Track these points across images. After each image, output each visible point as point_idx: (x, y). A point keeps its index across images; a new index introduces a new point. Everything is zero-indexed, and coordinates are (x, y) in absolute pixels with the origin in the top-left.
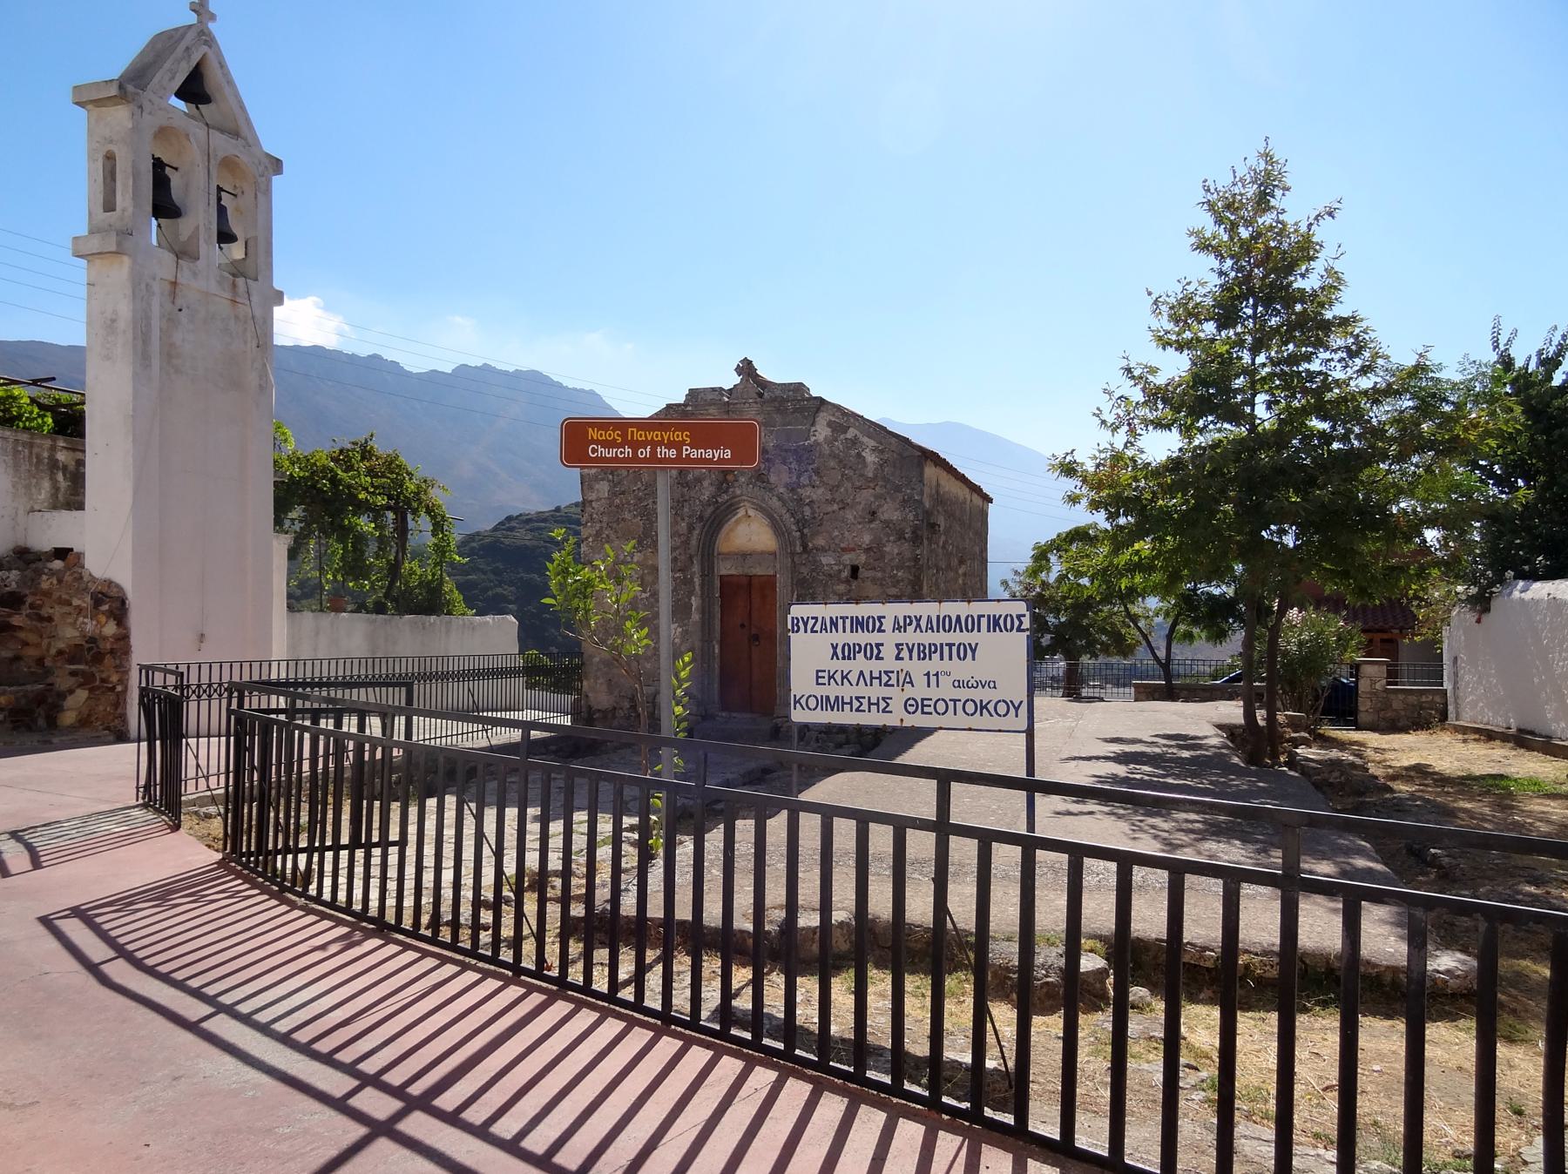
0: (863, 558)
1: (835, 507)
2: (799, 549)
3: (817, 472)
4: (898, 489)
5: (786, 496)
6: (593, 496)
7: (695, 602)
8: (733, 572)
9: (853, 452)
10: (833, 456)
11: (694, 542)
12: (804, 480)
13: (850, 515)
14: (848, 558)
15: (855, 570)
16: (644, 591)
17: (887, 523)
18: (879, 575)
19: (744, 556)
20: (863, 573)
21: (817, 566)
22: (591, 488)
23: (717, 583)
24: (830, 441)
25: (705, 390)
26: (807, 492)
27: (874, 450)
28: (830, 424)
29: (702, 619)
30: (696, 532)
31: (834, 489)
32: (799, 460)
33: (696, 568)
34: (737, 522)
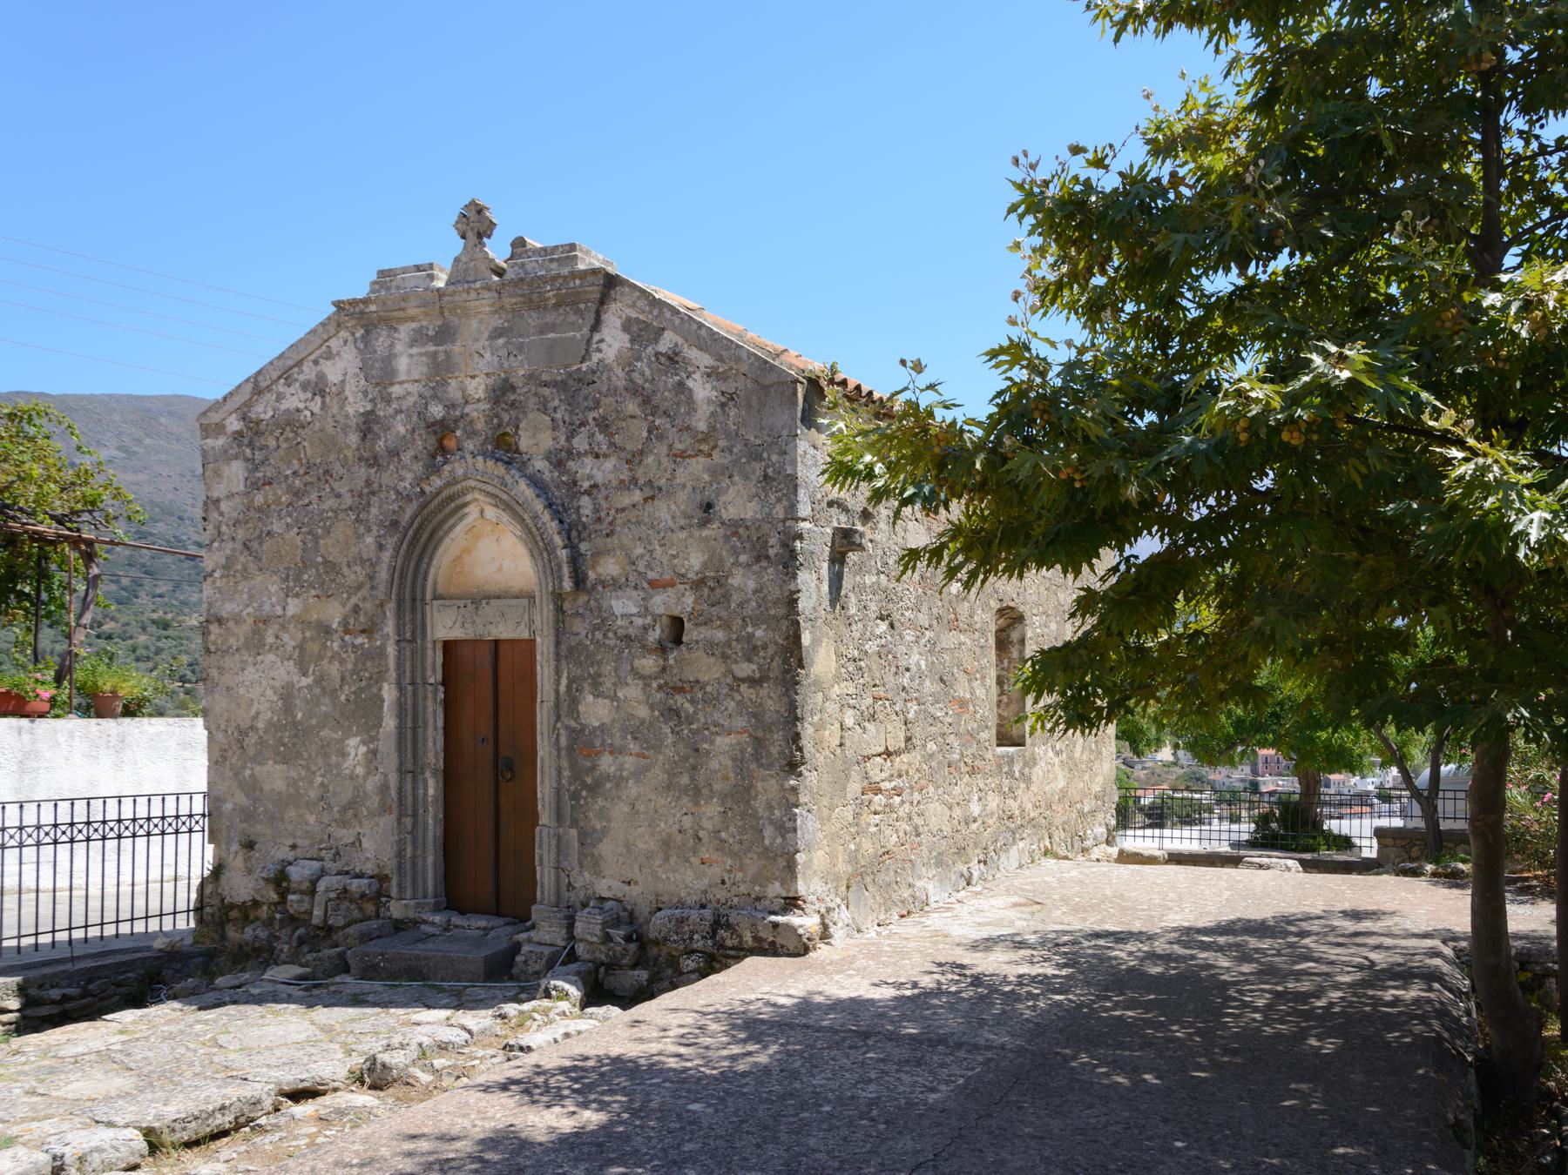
0: (689, 599)
1: (637, 496)
2: (568, 585)
3: (604, 425)
4: (755, 456)
5: (547, 476)
6: (219, 491)
7: (389, 693)
8: (457, 634)
10: (633, 390)
11: (383, 575)
12: (581, 443)
13: (663, 511)
14: (662, 603)
15: (677, 624)
17: (734, 527)
18: (720, 635)
19: (479, 599)
20: (691, 633)
21: (604, 622)
22: (218, 474)
24: (628, 363)
25: (405, 270)
26: (588, 470)
27: (710, 374)
28: (626, 327)
30: (386, 556)
31: (634, 459)
32: (571, 402)
33: (390, 628)
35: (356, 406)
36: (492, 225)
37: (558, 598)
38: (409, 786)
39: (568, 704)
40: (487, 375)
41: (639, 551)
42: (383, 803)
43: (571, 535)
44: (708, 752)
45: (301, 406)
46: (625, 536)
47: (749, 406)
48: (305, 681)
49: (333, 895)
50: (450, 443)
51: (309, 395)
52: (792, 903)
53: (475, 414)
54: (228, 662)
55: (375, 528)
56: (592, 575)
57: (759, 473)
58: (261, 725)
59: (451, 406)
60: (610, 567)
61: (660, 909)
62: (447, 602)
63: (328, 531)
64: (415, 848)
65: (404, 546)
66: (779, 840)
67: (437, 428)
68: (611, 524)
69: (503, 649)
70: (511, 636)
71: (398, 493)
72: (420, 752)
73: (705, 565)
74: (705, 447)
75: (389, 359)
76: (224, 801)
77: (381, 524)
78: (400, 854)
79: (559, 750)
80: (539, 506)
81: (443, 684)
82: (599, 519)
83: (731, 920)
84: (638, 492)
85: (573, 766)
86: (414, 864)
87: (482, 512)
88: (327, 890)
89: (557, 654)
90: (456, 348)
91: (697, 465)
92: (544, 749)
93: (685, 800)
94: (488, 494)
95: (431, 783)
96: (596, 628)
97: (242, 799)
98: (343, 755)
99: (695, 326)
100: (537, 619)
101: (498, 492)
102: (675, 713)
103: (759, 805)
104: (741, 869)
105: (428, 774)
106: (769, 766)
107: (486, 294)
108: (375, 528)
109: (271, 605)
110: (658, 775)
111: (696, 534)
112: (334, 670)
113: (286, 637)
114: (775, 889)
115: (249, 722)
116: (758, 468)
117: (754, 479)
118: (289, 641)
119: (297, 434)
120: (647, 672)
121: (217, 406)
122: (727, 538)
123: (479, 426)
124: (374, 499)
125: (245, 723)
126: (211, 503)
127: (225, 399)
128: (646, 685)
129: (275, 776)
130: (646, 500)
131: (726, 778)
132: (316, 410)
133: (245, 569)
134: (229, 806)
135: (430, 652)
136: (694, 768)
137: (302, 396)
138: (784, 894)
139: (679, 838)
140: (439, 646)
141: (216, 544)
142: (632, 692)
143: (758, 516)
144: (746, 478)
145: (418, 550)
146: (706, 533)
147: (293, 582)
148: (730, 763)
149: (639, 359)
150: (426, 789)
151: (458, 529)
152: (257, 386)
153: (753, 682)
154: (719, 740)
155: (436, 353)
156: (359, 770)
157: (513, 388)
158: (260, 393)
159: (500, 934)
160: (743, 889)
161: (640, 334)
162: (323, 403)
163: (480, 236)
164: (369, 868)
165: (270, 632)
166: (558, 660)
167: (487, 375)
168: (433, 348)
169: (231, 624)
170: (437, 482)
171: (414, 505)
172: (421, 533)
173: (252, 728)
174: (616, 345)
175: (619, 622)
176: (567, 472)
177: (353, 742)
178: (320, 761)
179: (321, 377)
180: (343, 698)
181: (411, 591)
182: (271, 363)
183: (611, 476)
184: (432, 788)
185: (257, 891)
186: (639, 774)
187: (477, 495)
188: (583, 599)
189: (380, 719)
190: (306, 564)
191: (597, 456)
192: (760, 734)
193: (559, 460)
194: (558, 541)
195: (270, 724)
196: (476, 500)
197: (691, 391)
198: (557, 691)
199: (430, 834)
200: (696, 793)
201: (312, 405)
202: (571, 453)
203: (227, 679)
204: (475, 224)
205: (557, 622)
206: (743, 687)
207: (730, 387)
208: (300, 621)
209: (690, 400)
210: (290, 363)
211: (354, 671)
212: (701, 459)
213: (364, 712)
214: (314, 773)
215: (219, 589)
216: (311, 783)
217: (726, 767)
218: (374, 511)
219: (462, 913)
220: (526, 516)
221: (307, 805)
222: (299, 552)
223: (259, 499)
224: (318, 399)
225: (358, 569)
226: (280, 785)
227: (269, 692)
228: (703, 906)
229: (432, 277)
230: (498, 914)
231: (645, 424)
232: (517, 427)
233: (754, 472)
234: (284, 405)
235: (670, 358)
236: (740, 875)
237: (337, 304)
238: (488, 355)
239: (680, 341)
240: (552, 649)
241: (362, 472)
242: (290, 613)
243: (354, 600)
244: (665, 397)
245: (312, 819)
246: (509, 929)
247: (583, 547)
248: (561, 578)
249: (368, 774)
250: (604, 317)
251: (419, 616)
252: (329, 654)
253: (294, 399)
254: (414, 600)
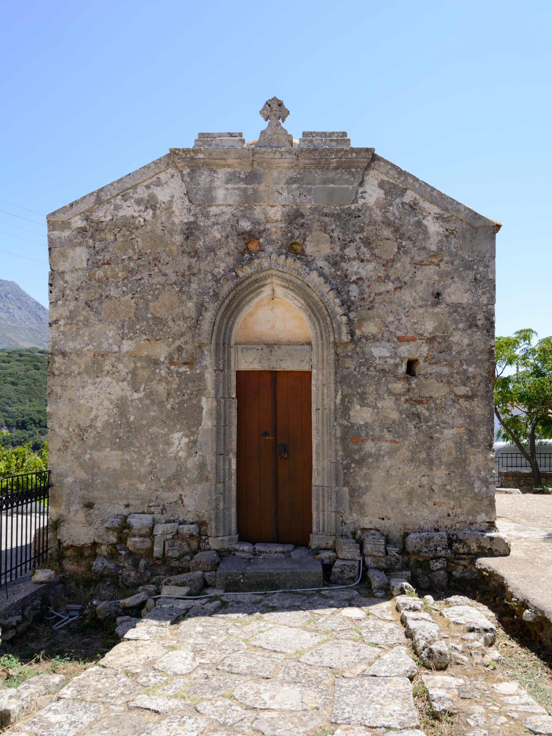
1: (390, 286)
3: (367, 242)
10: (388, 223)
12: (350, 252)
14: (406, 351)
17: (455, 308)
24: (384, 207)
26: (354, 268)
32: (344, 228)
41: (391, 319)
46: (380, 310)
47: (464, 238)
48: (136, 396)
57: (471, 277)
58: (99, 424)
60: (370, 328)
68: (371, 302)
73: (435, 329)
74: (435, 260)
84: (391, 284)
99: (429, 189)
111: (430, 310)
115: (88, 423)
116: (471, 275)
117: (468, 281)
122: (450, 314)
130: (396, 289)
143: (471, 302)
144: (463, 279)
146: (436, 310)
149: (391, 205)
173: (90, 426)
174: (375, 196)
183: (372, 274)
197: (426, 227)
207: (451, 226)
212: (433, 267)
231: (396, 244)
232: (305, 240)
235: (411, 206)
239: (418, 197)
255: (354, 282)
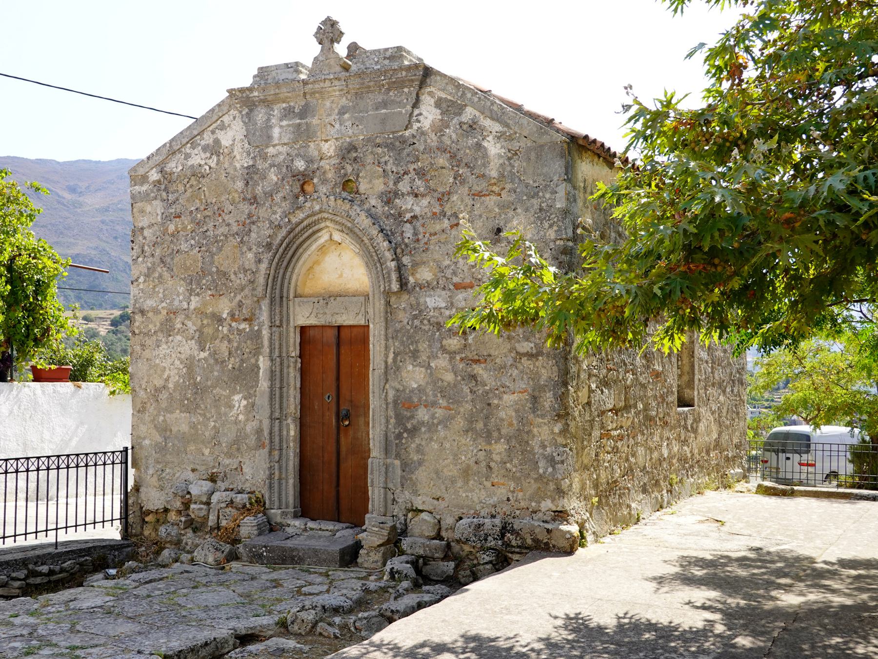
1: (446, 223)
2: (395, 286)
3: (421, 173)
5: (379, 210)
6: (144, 222)
7: (263, 363)
8: (312, 321)
9: (471, 142)
11: (261, 280)
12: (404, 187)
16: (203, 350)
19: (329, 297)
23: (294, 339)
24: (439, 129)
25: (277, 67)
26: (408, 204)
27: (499, 137)
28: (438, 104)
29: (272, 388)
30: (263, 266)
33: (264, 316)
34: (322, 249)
35: (242, 161)
36: (342, 33)
37: (388, 294)
38: (276, 429)
39: (391, 371)
40: (336, 139)
41: (447, 262)
42: (259, 439)
43: (396, 253)
44: (498, 406)
45: (203, 162)
46: (436, 252)
48: (203, 355)
49: (223, 505)
50: (308, 188)
51: (208, 155)
52: (561, 515)
53: (328, 167)
54: (149, 342)
55: (254, 248)
56: (411, 280)
57: (536, 207)
58: (171, 385)
59: (310, 161)
60: (425, 274)
61: (461, 518)
62: (305, 299)
63: (220, 249)
64: (280, 472)
65: (276, 260)
66: (550, 470)
67: (300, 177)
68: (426, 243)
69: (344, 334)
70: (351, 323)
71: (271, 222)
72: (285, 405)
74: (496, 189)
75: (268, 127)
76: (144, 439)
77: (259, 245)
78: (271, 476)
79: (387, 404)
80: (374, 231)
81: (300, 357)
82: (418, 240)
83: (515, 527)
84: (446, 221)
85: (398, 416)
86: (280, 484)
87: (331, 235)
88: (219, 502)
89: (386, 335)
90: (315, 121)
91: (491, 201)
92: (375, 402)
93: (480, 440)
94: (336, 222)
95: (292, 427)
96: (415, 317)
97: (159, 439)
98: (231, 407)
99: (489, 103)
100: (371, 311)
101: (344, 221)
102: (474, 377)
103: (535, 443)
104: (521, 490)
105: (289, 421)
106: (543, 416)
107: (336, 83)
108: (254, 248)
109: (179, 302)
110: (460, 423)
112: (224, 347)
113: (189, 324)
114: (547, 505)
118: (191, 327)
119: (199, 182)
120: (453, 348)
121: (141, 163)
123: (330, 175)
124: (254, 227)
125: (159, 383)
126: (137, 231)
127: (148, 158)
128: (451, 359)
129: (180, 421)
130: (452, 227)
131: (511, 424)
132: (213, 165)
133: (161, 276)
134: (147, 442)
135: (292, 335)
136: (487, 417)
137: (203, 156)
138: (554, 509)
139: (475, 467)
140: (298, 330)
141: (140, 259)
142: (441, 362)
145: (285, 263)
147: (194, 283)
148: (514, 414)
149: (448, 127)
150: (288, 432)
151: (314, 247)
152: (172, 149)
153: (530, 356)
154: (505, 396)
155: (299, 125)
156: (241, 417)
157: (355, 149)
158: (174, 153)
159: (344, 535)
160: (523, 504)
161: (450, 108)
162: (218, 161)
163: (332, 41)
164: (247, 487)
165: (179, 320)
166: (387, 339)
167: (336, 139)
168: (298, 121)
169: (150, 314)
170: (301, 215)
171: (283, 232)
172: (288, 250)
173: (164, 387)
174: (431, 117)
175: (431, 314)
176: (395, 207)
177: (237, 397)
178: (213, 411)
179: (217, 142)
180: (230, 366)
181: (279, 293)
182: (181, 133)
184: (293, 431)
185: (168, 502)
186: (445, 422)
187: (328, 223)
188: (405, 297)
189: (257, 381)
190: (204, 272)
191: (416, 196)
192: (537, 394)
193: (389, 197)
194: (388, 255)
195: (177, 384)
196: (327, 227)
197: (485, 149)
198: (386, 362)
199: (291, 464)
200: (488, 436)
201: (210, 162)
202: (396, 194)
203: (147, 353)
204: (329, 32)
205: (387, 312)
206: (524, 360)
207: (515, 145)
208: (200, 312)
209: (485, 155)
210: (195, 132)
211: (237, 348)
212: (494, 198)
213: (244, 377)
214: (208, 419)
215: (142, 290)
216: (206, 426)
217: (511, 417)
218: (253, 235)
219: (313, 519)
220: (364, 238)
221: (203, 442)
222: (200, 264)
223: (172, 228)
224: (215, 158)
225: (242, 276)
226: (185, 428)
227: (177, 362)
228: (493, 517)
229: (298, 72)
230: (339, 521)
231: (452, 173)
232: (358, 176)
233: (533, 206)
234: (190, 162)
235: (471, 126)
236: (520, 495)
237: (228, 91)
238: (337, 126)
239: (478, 114)
240: (383, 333)
241: (245, 208)
242: (192, 307)
243: (239, 298)
244: (467, 154)
245: (207, 452)
246: (350, 531)
247: (406, 260)
248: (390, 281)
249: (247, 420)
250: (422, 98)
251: (285, 309)
252: (221, 336)
253: (197, 158)
254: (281, 298)
255: (409, 222)
